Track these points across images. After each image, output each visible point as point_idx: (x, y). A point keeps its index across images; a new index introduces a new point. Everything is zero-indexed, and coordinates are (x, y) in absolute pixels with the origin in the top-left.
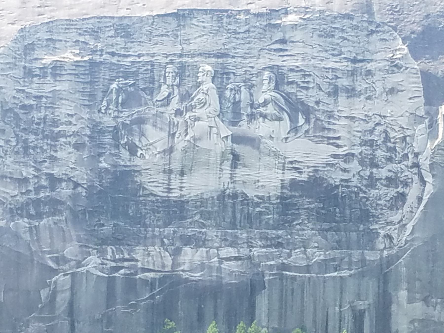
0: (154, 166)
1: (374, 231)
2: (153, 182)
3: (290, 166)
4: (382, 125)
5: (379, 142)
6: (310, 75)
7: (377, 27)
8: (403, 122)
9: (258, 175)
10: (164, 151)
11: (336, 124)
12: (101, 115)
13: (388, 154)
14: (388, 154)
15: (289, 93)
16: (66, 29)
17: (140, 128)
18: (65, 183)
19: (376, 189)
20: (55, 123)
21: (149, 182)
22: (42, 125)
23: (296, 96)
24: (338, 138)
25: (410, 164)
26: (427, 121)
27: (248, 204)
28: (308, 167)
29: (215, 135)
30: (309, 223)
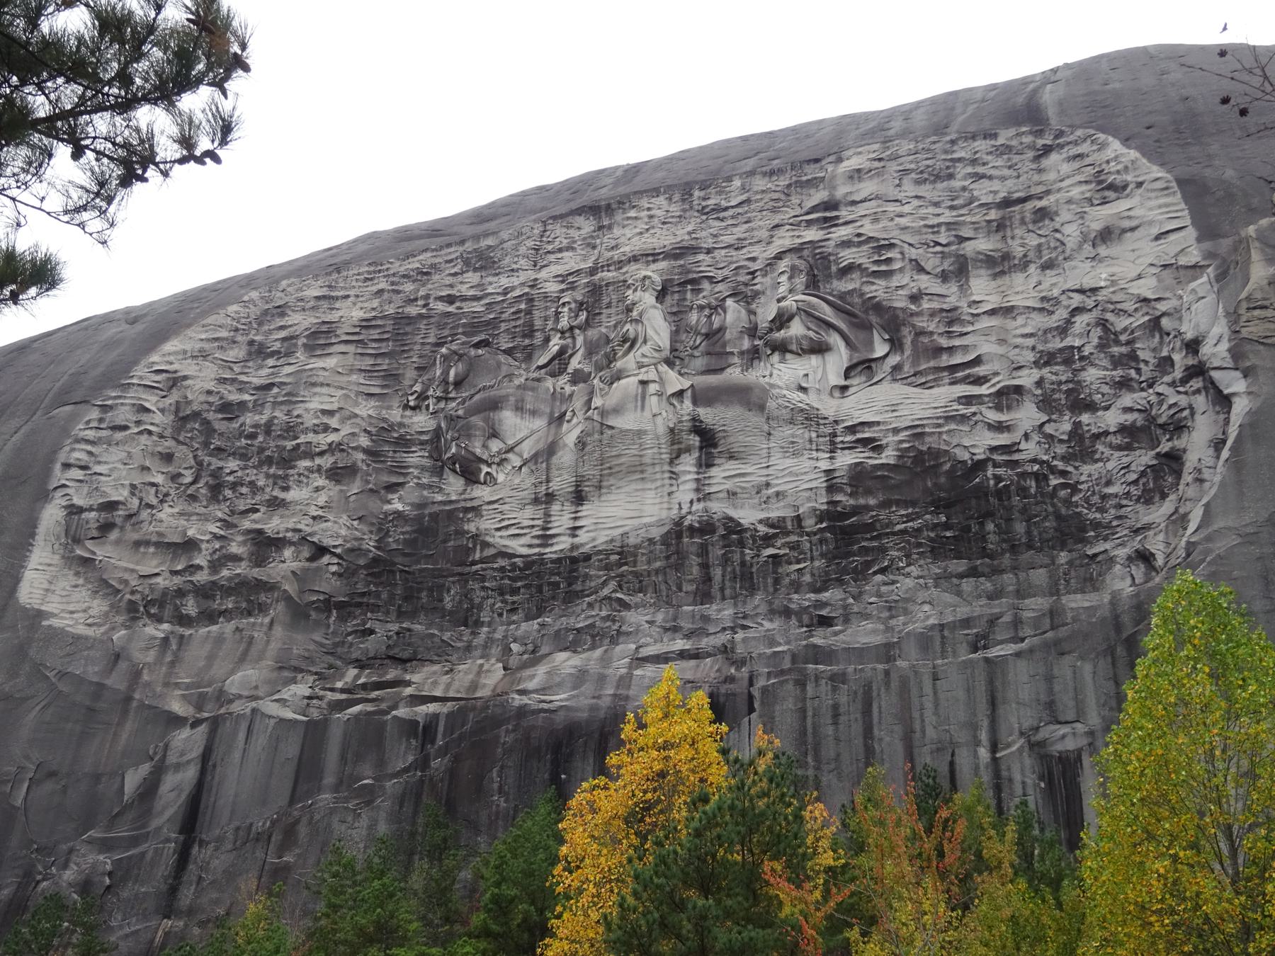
0: (514, 493)
1: (1099, 559)
2: (507, 527)
3: (849, 438)
4: (1090, 310)
5: (1087, 351)
6: (892, 246)
7: (1057, 137)
8: (1146, 288)
9: (765, 472)
10: (535, 457)
11: (966, 334)
12: (408, 413)
13: (1118, 373)
14: (1118, 373)
15: (845, 293)
16: (366, 279)
17: (486, 420)
18: (293, 548)
19: (1096, 461)
20: (291, 430)
21: (498, 529)
22: (260, 438)
23: (862, 295)
24: (977, 361)
25: (1178, 374)
26: (1210, 270)
27: (741, 544)
28: (896, 431)
29: (654, 399)
30: (908, 565)
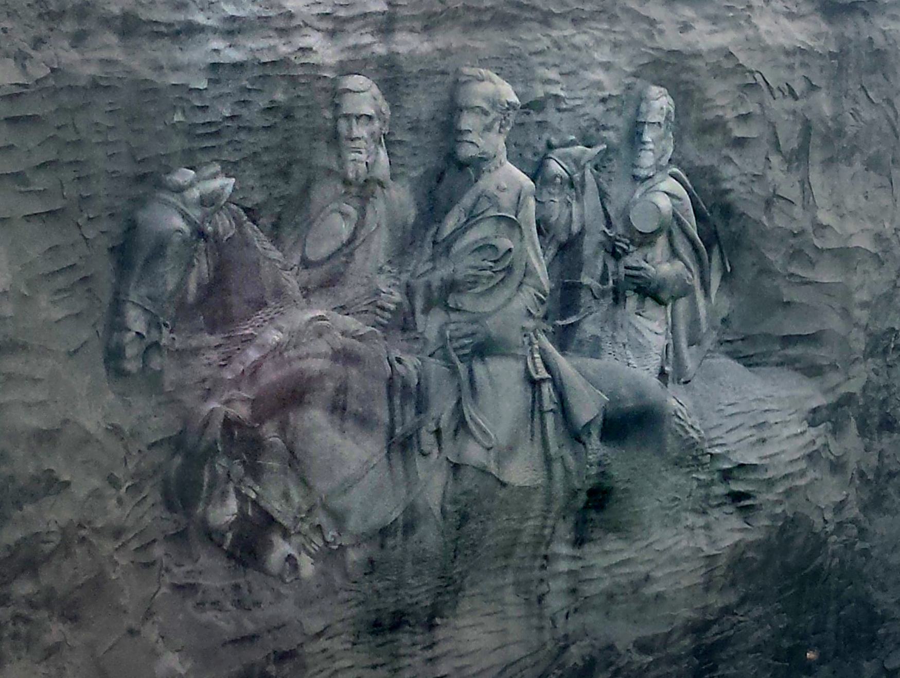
17: (283, 429)
23: (715, 181)
29: (550, 419)
